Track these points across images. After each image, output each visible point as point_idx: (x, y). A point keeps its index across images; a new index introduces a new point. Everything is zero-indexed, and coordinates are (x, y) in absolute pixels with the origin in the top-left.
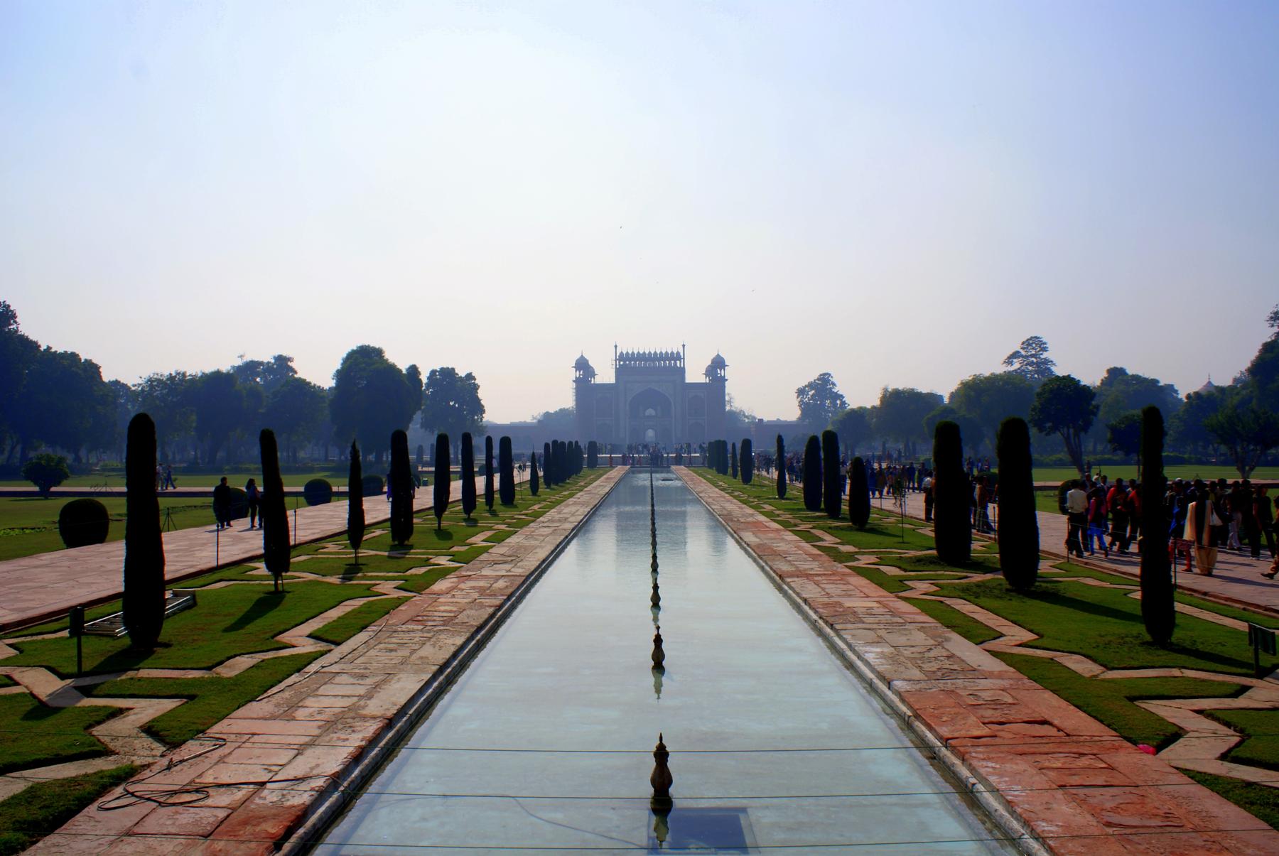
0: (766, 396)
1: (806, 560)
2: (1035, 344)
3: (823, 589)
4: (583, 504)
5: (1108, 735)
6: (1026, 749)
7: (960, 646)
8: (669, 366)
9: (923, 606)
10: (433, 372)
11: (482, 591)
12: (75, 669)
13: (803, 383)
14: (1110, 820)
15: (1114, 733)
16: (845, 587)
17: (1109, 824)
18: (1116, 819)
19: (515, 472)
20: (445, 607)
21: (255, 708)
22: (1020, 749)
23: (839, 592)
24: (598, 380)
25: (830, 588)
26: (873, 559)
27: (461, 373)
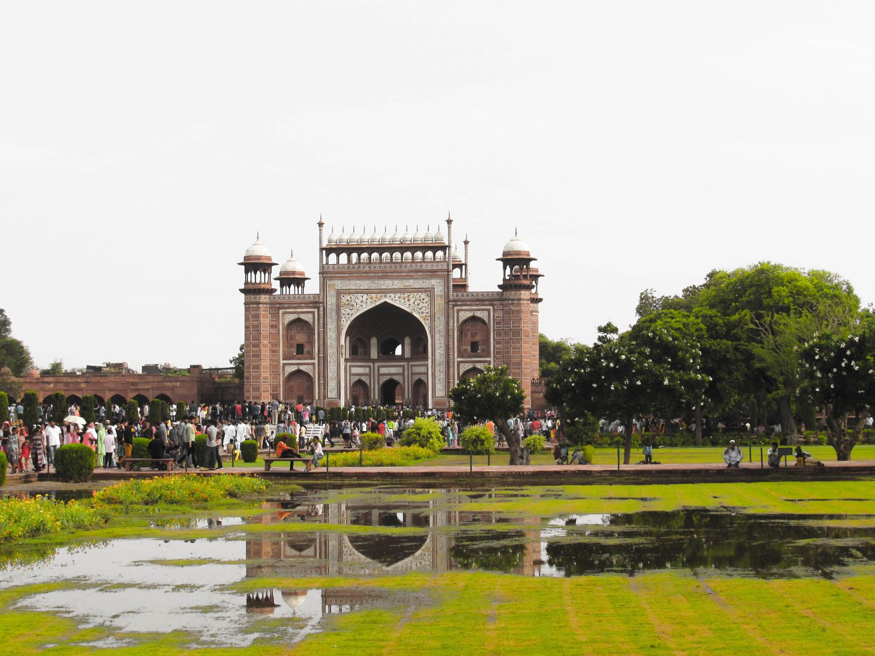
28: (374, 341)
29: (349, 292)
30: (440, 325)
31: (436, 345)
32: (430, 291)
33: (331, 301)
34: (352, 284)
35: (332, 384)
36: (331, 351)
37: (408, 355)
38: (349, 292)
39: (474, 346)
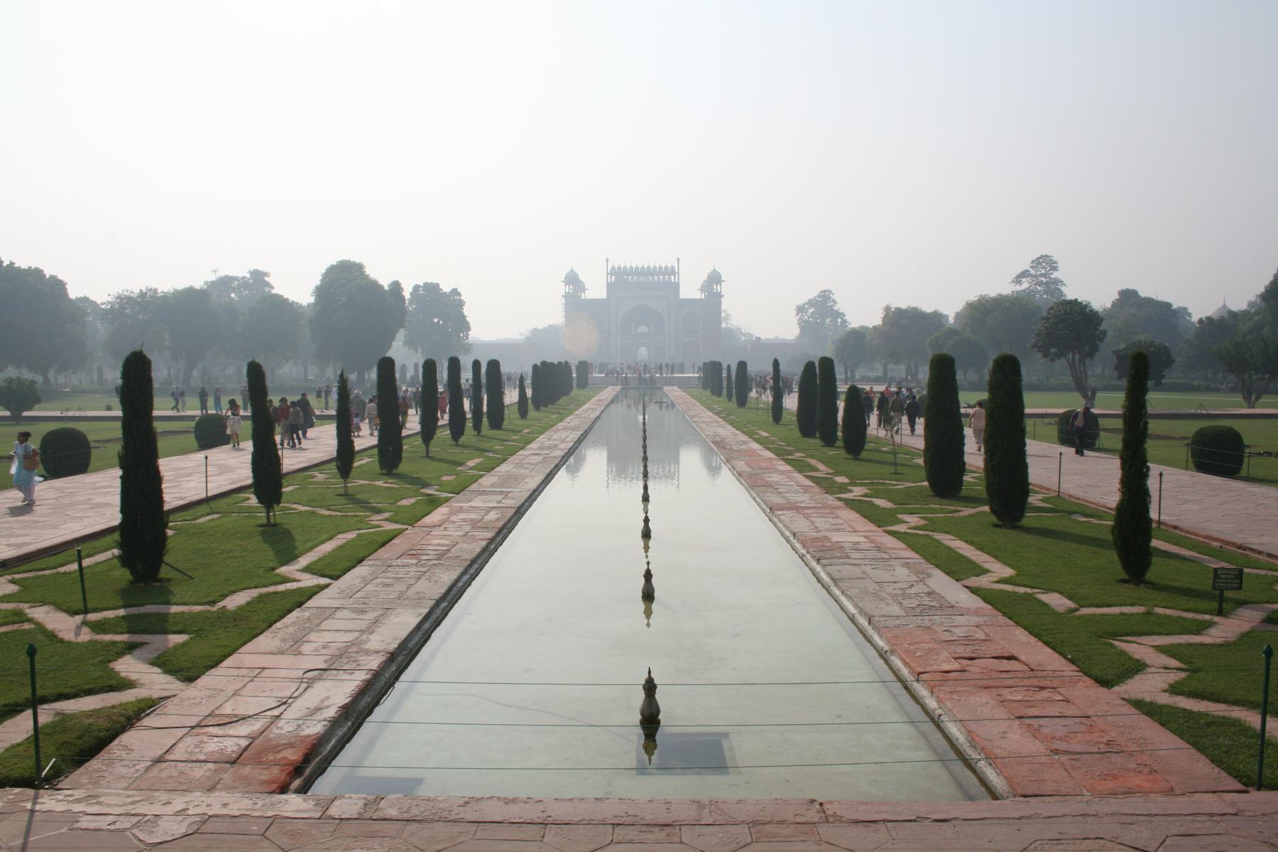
2: (1046, 263)
3: (813, 523)
4: (573, 429)
5: (1069, 670)
6: (991, 683)
7: (941, 582)
9: (907, 539)
10: (416, 287)
11: (474, 524)
12: (81, 606)
13: (803, 300)
14: (1057, 747)
15: (1075, 668)
16: (834, 521)
17: (1056, 752)
18: (1062, 746)
20: (437, 541)
21: (266, 641)
22: (986, 683)
23: (828, 526)
25: (820, 522)
27: (446, 288)
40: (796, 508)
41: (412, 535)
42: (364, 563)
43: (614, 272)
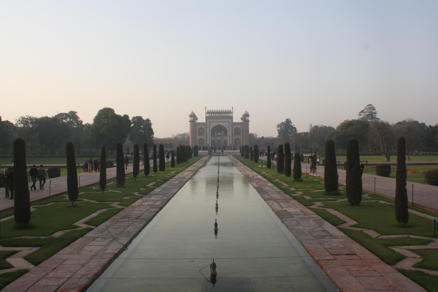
0: (264, 128)
1: (275, 194)
2: (371, 107)
3: (280, 205)
4: (191, 171)
7: (328, 226)
8: (226, 115)
9: (316, 211)
11: (151, 206)
13: (279, 123)
15: (378, 258)
16: (288, 204)
19: (166, 158)
20: (137, 212)
24: (198, 121)
25: (282, 204)
26: (301, 193)
27: (145, 118)
28: (216, 132)
29: (212, 122)
30: (231, 128)
31: (229, 133)
32: (229, 122)
33: (208, 124)
34: (212, 120)
35: (208, 141)
36: (208, 134)
37: (223, 135)
38: (212, 122)
39: (237, 133)
40: (275, 200)
41: (127, 211)
42: (108, 220)
43: (208, 113)
